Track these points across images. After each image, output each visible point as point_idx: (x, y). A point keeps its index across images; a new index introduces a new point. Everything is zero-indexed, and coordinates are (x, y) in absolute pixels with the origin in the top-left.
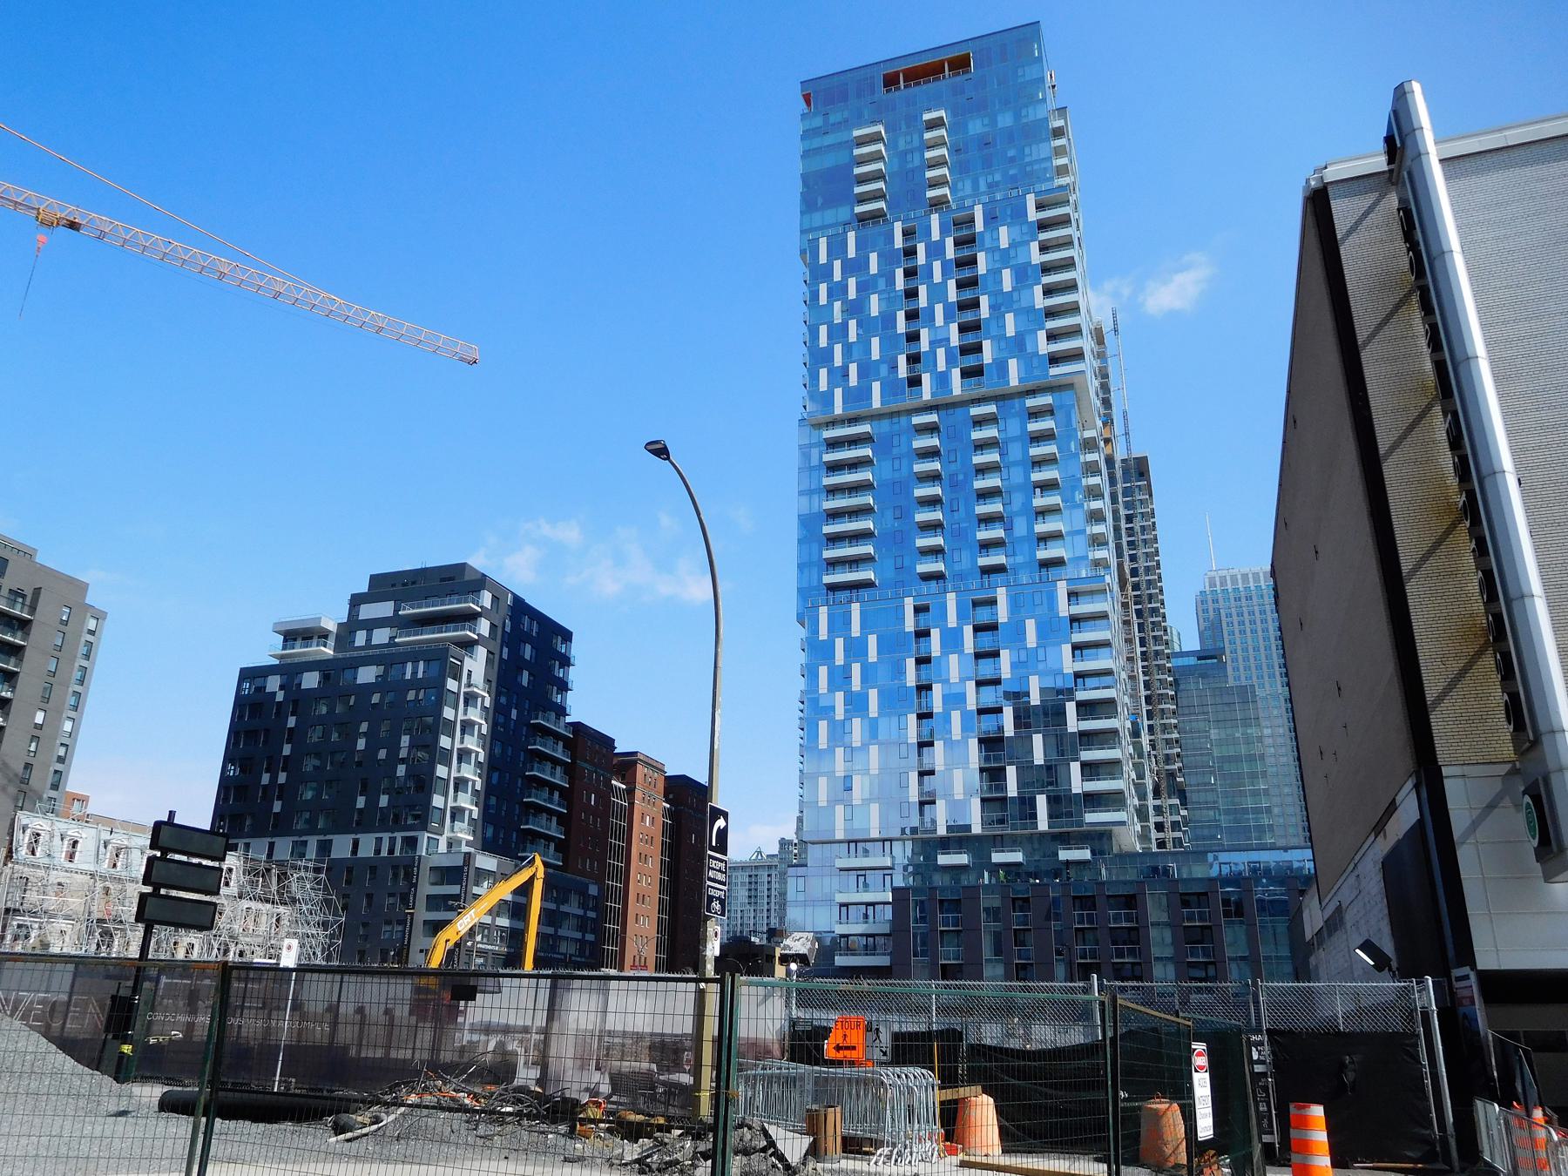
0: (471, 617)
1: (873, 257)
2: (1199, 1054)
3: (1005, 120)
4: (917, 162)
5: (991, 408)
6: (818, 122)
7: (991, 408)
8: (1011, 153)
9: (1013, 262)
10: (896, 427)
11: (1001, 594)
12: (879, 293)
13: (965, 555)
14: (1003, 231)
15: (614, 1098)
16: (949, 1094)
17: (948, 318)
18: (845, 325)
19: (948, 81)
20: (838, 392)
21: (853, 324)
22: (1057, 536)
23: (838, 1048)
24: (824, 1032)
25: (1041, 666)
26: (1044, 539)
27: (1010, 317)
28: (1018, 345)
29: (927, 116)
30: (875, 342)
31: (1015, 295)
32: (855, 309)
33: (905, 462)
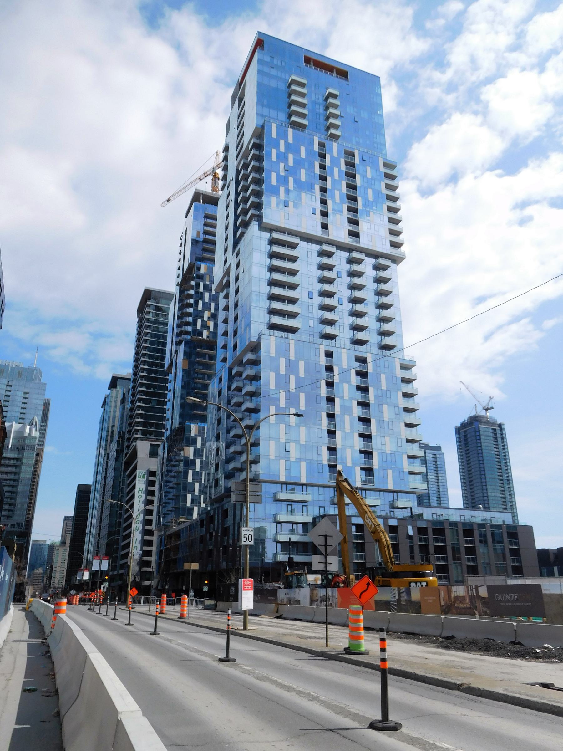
8: (367, 133)
14: (368, 169)
19: (334, 79)
21: (291, 180)
25: (388, 400)
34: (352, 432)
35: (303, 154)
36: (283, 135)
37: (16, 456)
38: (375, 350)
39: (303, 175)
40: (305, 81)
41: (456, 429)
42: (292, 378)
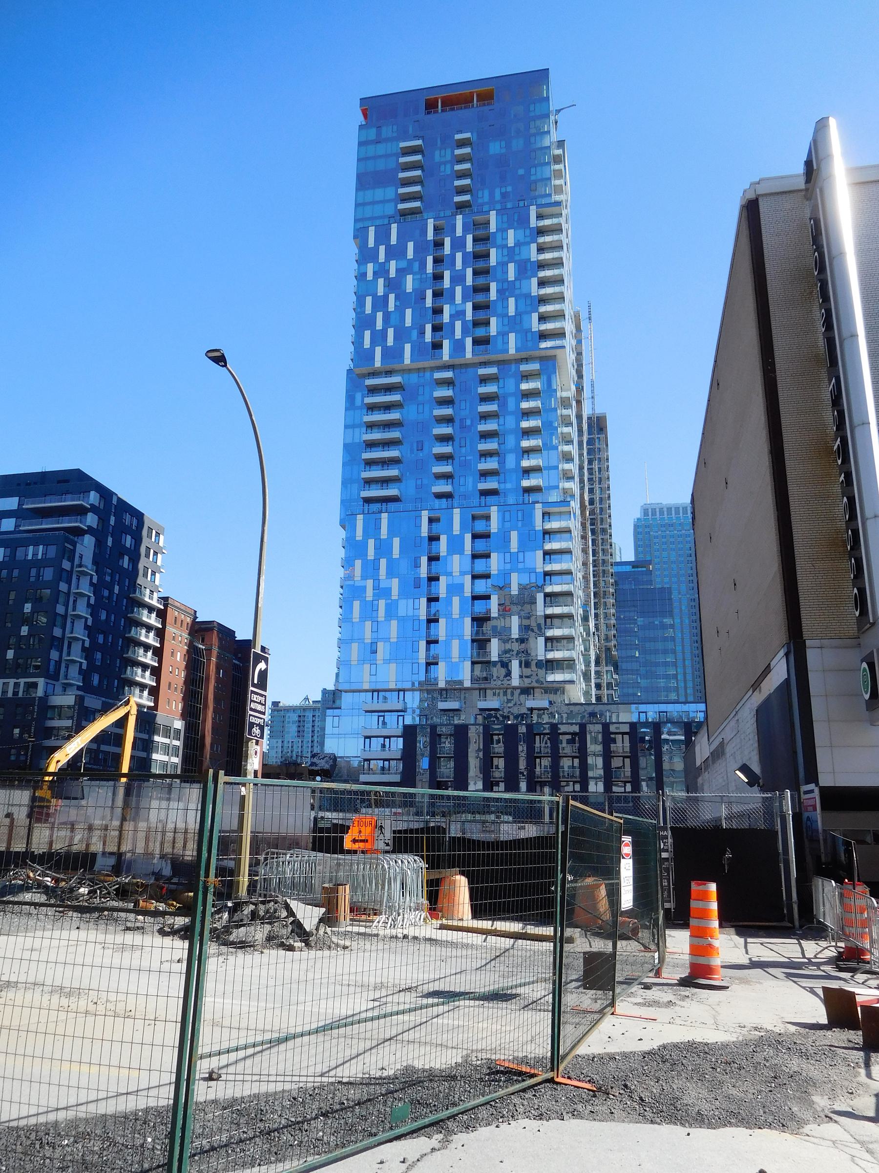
0: (80, 511)
1: (410, 246)
2: (627, 845)
3: (518, 144)
4: (448, 172)
5: (493, 370)
6: (372, 133)
7: (493, 370)
8: (521, 172)
9: (517, 258)
11: (494, 512)
13: (470, 480)
14: (511, 232)
15: (175, 880)
16: (435, 874)
17: (465, 299)
18: (386, 298)
20: (378, 350)
21: (392, 297)
22: (537, 469)
23: (355, 841)
24: (344, 829)
25: (521, 566)
26: (527, 472)
27: (512, 301)
28: (515, 324)
29: (458, 137)
30: (409, 312)
32: (394, 285)
33: (427, 407)
35: (410, 254)
36: (383, 236)
40: (419, 142)
42: (383, 562)
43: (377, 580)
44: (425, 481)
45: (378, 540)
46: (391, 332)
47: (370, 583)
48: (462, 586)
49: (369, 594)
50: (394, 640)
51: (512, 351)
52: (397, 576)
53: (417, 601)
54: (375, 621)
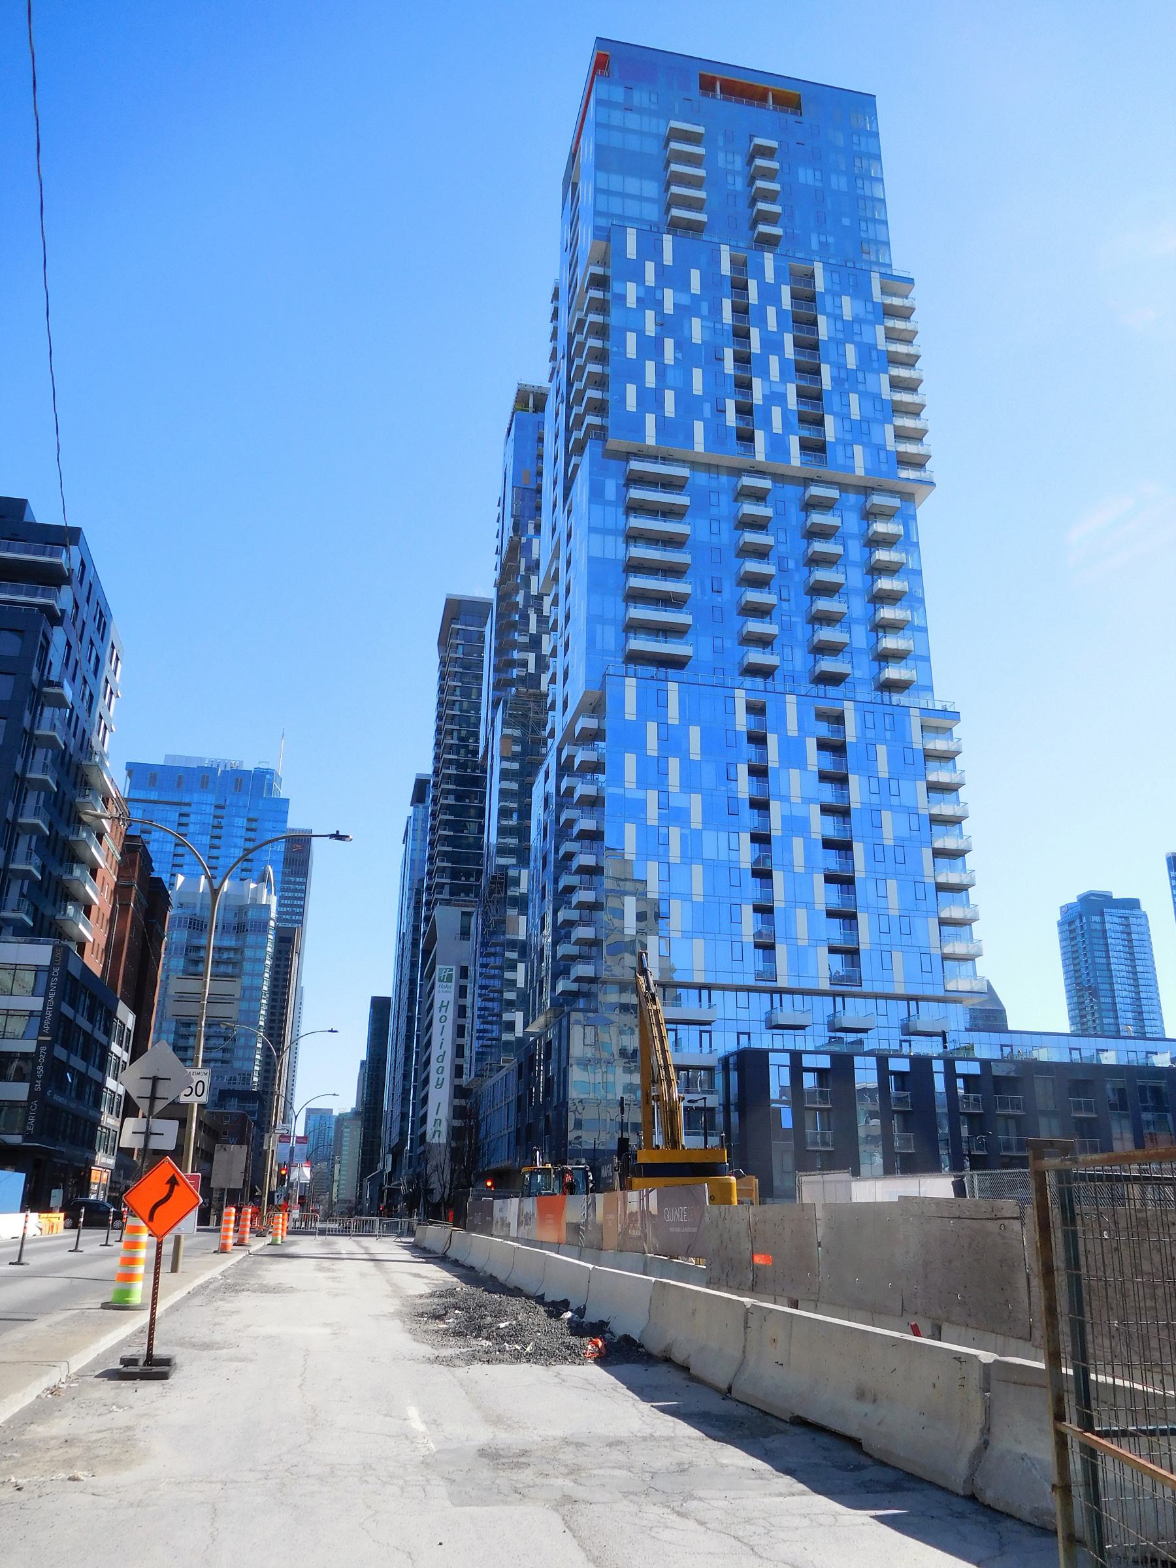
8: (846, 221)
9: (857, 338)
10: (714, 483)
11: (849, 709)
12: (702, 318)
17: (784, 378)
19: (768, 115)
20: (650, 420)
21: (669, 344)
25: (895, 801)
27: (854, 398)
29: (758, 141)
30: (697, 374)
31: (860, 375)
34: (810, 868)
35: (696, 286)
36: (649, 249)
37: (233, 944)
38: (866, 693)
39: (697, 330)
40: (701, 130)
41: (1168, 859)
42: (674, 764)
43: (664, 792)
44: (728, 644)
45: (663, 724)
46: (670, 396)
47: (652, 796)
48: (806, 820)
49: (652, 814)
50: (698, 899)
51: (860, 472)
52: (699, 790)
53: (733, 836)
54: (664, 862)
